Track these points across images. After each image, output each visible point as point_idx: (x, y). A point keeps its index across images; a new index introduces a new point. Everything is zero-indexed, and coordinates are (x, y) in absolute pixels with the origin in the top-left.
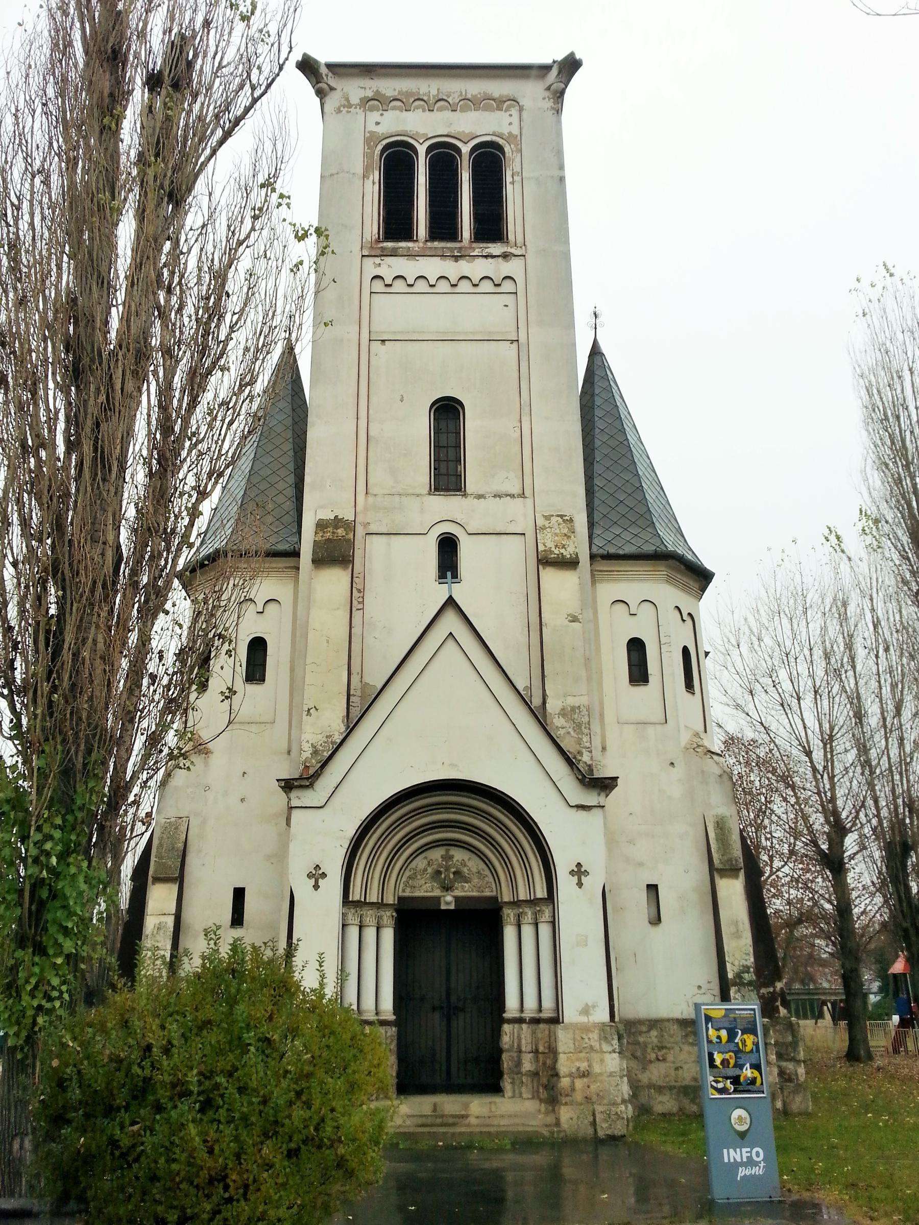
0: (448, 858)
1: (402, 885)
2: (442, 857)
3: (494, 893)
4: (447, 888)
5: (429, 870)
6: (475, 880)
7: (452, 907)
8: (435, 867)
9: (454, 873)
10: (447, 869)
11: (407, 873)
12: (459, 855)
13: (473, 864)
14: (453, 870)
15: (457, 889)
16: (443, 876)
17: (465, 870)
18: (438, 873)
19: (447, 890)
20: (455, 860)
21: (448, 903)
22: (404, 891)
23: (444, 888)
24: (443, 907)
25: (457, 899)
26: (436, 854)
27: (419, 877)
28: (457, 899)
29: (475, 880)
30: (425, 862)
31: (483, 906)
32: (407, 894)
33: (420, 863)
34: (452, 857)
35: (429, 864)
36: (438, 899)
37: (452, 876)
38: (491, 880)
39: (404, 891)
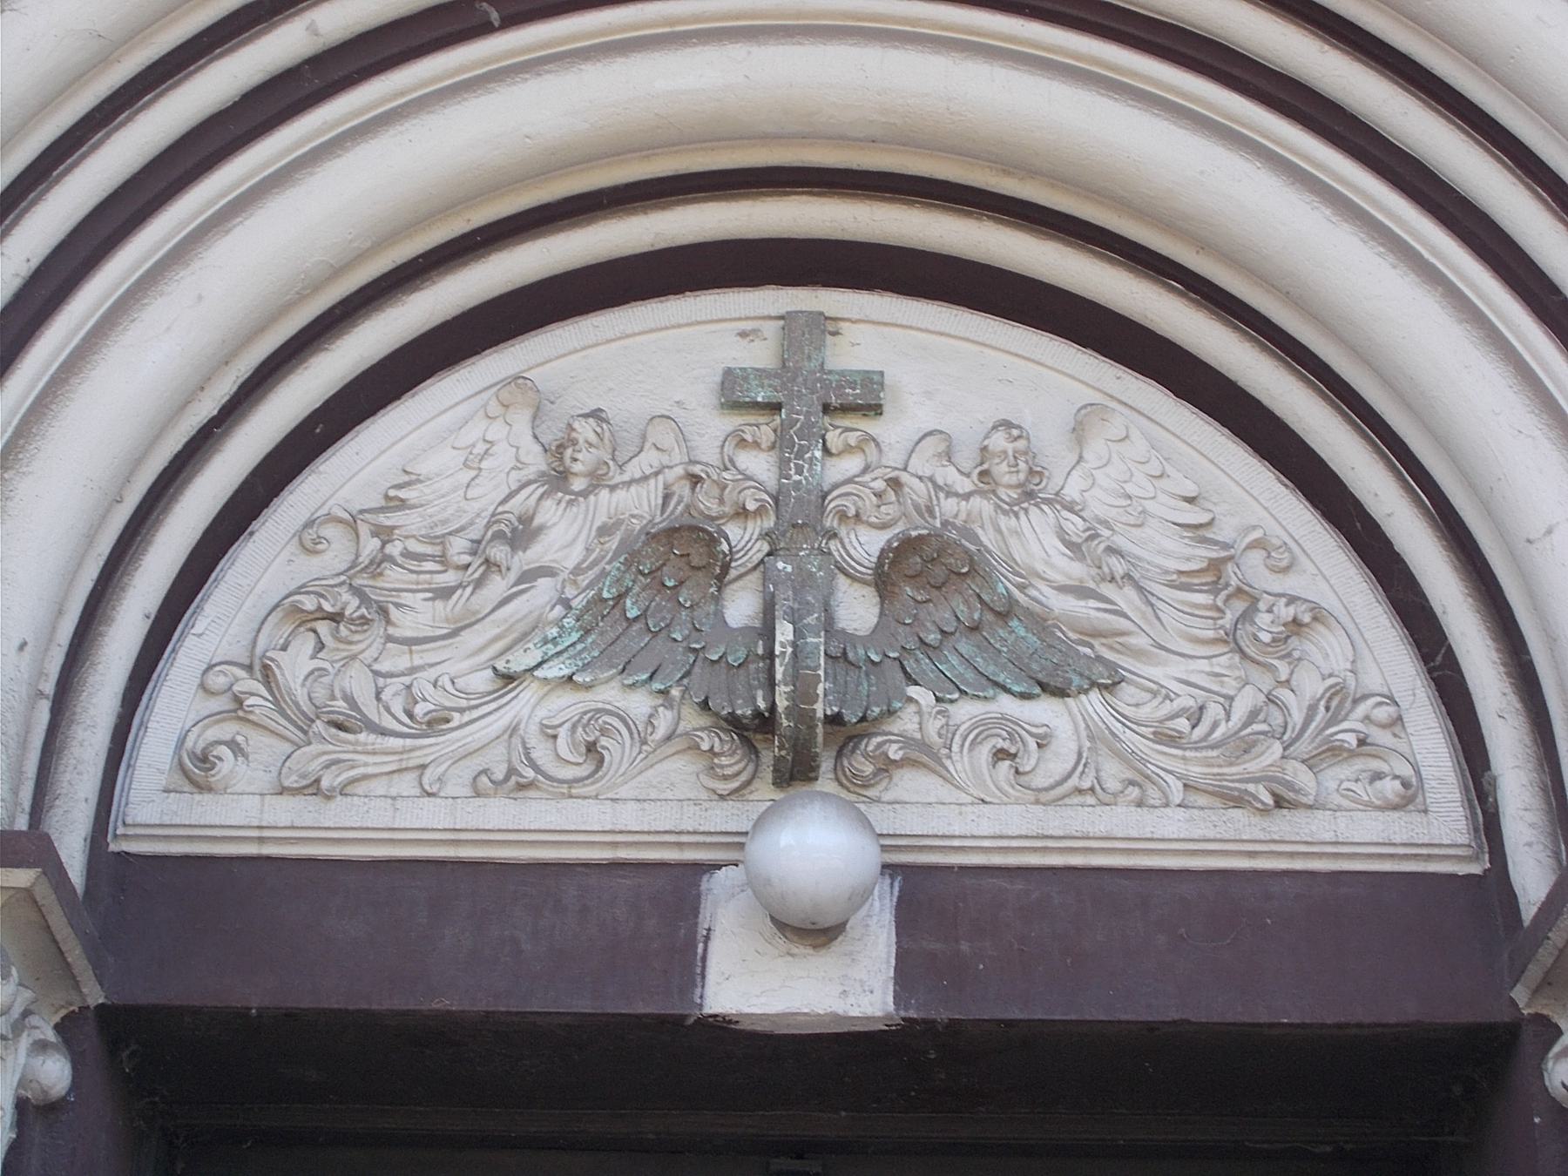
0: (811, 404)
1: (175, 704)
2: (734, 395)
3: (1438, 831)
4: (790, 742)
5: (566, 536)
6: (1177, 664)
7: (853, 988)
8: (637, 504)
9: (885, 577)
10: (801, 520)
11: (263, 565)
12: (947, 387)
13: (1134, 477)
14: (866, 545)
15: (923, 756)
16: (741, 607)
17: (1032, 550)
18: (683, 550)
19: (796, 771)
20: (892, 432)
21: (813, 931)
22: (196, 771)
23: (752, 730)
24: (748, 983)
25: (928, 896)
26: (666, 368)
27: (418, 615)
28: (928, 896)
29: (1177, 664)
30: (515, 448)
31: (1286, 1001)
32: (249, 810)
33: (447, 446)
34: (863, 400)
35: (557, 479)
36: (666, 897)
37: (857, 610)
38: (1393, 663)
39: (196, 771)
